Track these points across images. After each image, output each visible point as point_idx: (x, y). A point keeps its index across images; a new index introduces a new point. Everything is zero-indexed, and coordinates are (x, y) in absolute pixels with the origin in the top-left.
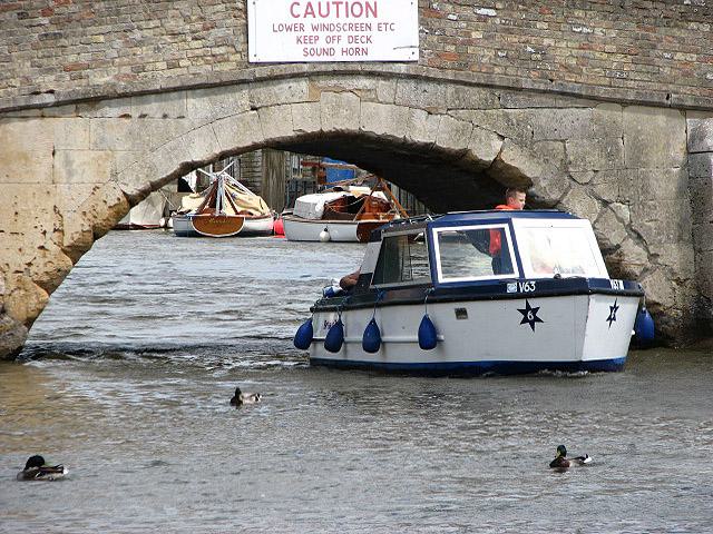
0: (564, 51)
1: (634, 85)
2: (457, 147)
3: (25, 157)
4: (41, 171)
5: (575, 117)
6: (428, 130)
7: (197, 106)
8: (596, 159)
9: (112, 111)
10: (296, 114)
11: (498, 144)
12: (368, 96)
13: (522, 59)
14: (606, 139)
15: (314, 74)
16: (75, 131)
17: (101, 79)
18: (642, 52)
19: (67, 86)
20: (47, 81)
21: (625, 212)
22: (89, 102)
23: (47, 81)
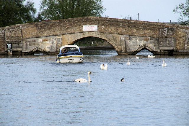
0: (110, 30)
1: (116, 32)
2: (101, 38)
3: (65, 38)
4: (66, 40)
5: (111, 35)
6: (98, 36)
7: (79, 34)
8: (112, 39)
9: (72, 34)
10: (87, 35)
11: (104, 37)
12: (93, 33)
13: (106, 30)
14: (113, 37)
15: (89, 32)
16: (69, 36)
17: (71, 32)
18: (116, 30)
19: (68, 32)
20: (67, 32)
21: (115, 43)
22: (70, 34)
23: (67, 32)
